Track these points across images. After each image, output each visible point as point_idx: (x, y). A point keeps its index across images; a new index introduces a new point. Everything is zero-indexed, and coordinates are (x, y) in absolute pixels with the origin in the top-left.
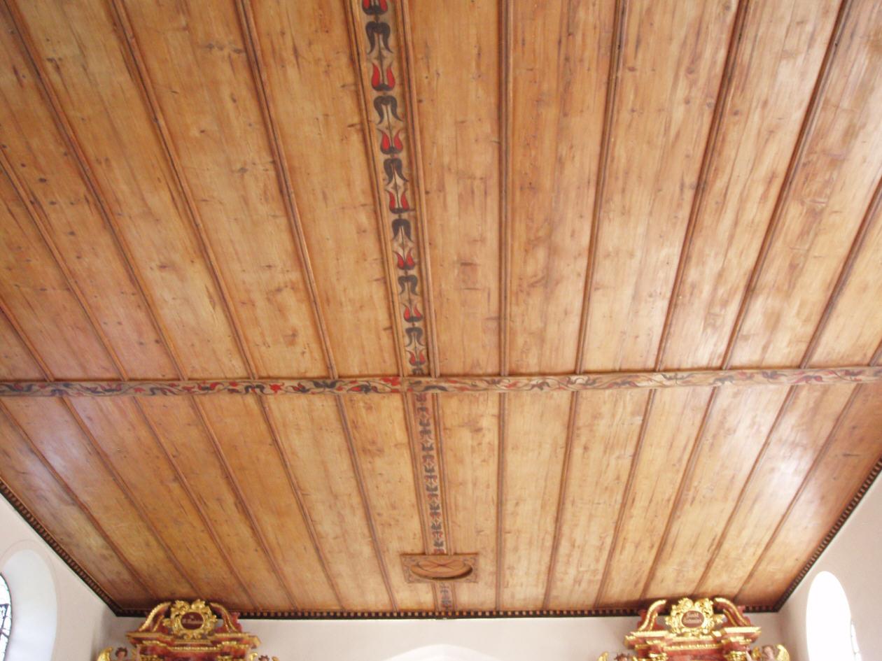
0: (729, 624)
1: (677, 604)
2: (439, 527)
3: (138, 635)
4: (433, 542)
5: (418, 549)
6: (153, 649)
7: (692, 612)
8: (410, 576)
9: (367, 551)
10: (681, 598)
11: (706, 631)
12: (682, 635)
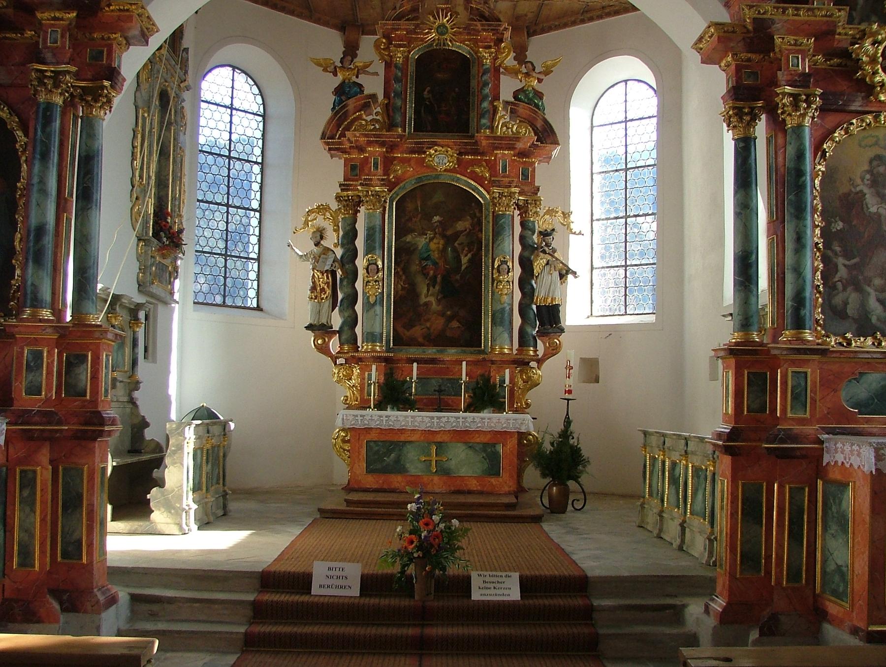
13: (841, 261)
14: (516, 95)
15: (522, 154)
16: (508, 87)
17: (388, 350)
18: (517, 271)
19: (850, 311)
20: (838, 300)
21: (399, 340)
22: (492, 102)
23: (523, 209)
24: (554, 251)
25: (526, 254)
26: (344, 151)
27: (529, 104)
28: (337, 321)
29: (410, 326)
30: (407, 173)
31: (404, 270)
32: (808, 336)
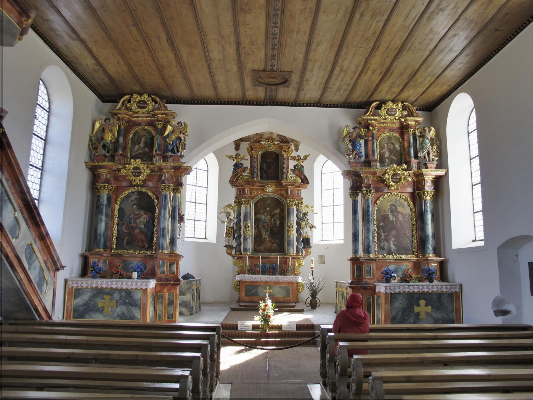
0: (409, 115)
1: (385, 104)
2: (275, 56)
3: (115, 112)
4: (270, 64)
5: (262, 68)
6: (123, 118)
7: (392, 108)
8: (255, 82)
9: (235, 68)
10: (388, 101)
11: (397, 118)
12: (386, 119)
13: (382, 234)
14: (295, 166)
15: (297, 187)
16: (292, 164)
17: (252, 254)
18: (296, 226)
19: (385, 248)
20: (382, 245)
21: (256, 251)
22: (286, 169)
23: (297, 205)
24: (308, 220)
25: (298, 221)
26: (237, 186)
27: (299, 170)
28: (234, 244)
29: (259, 245)
30: (258, 194)
31: (257, 227)
32: (371, 256)
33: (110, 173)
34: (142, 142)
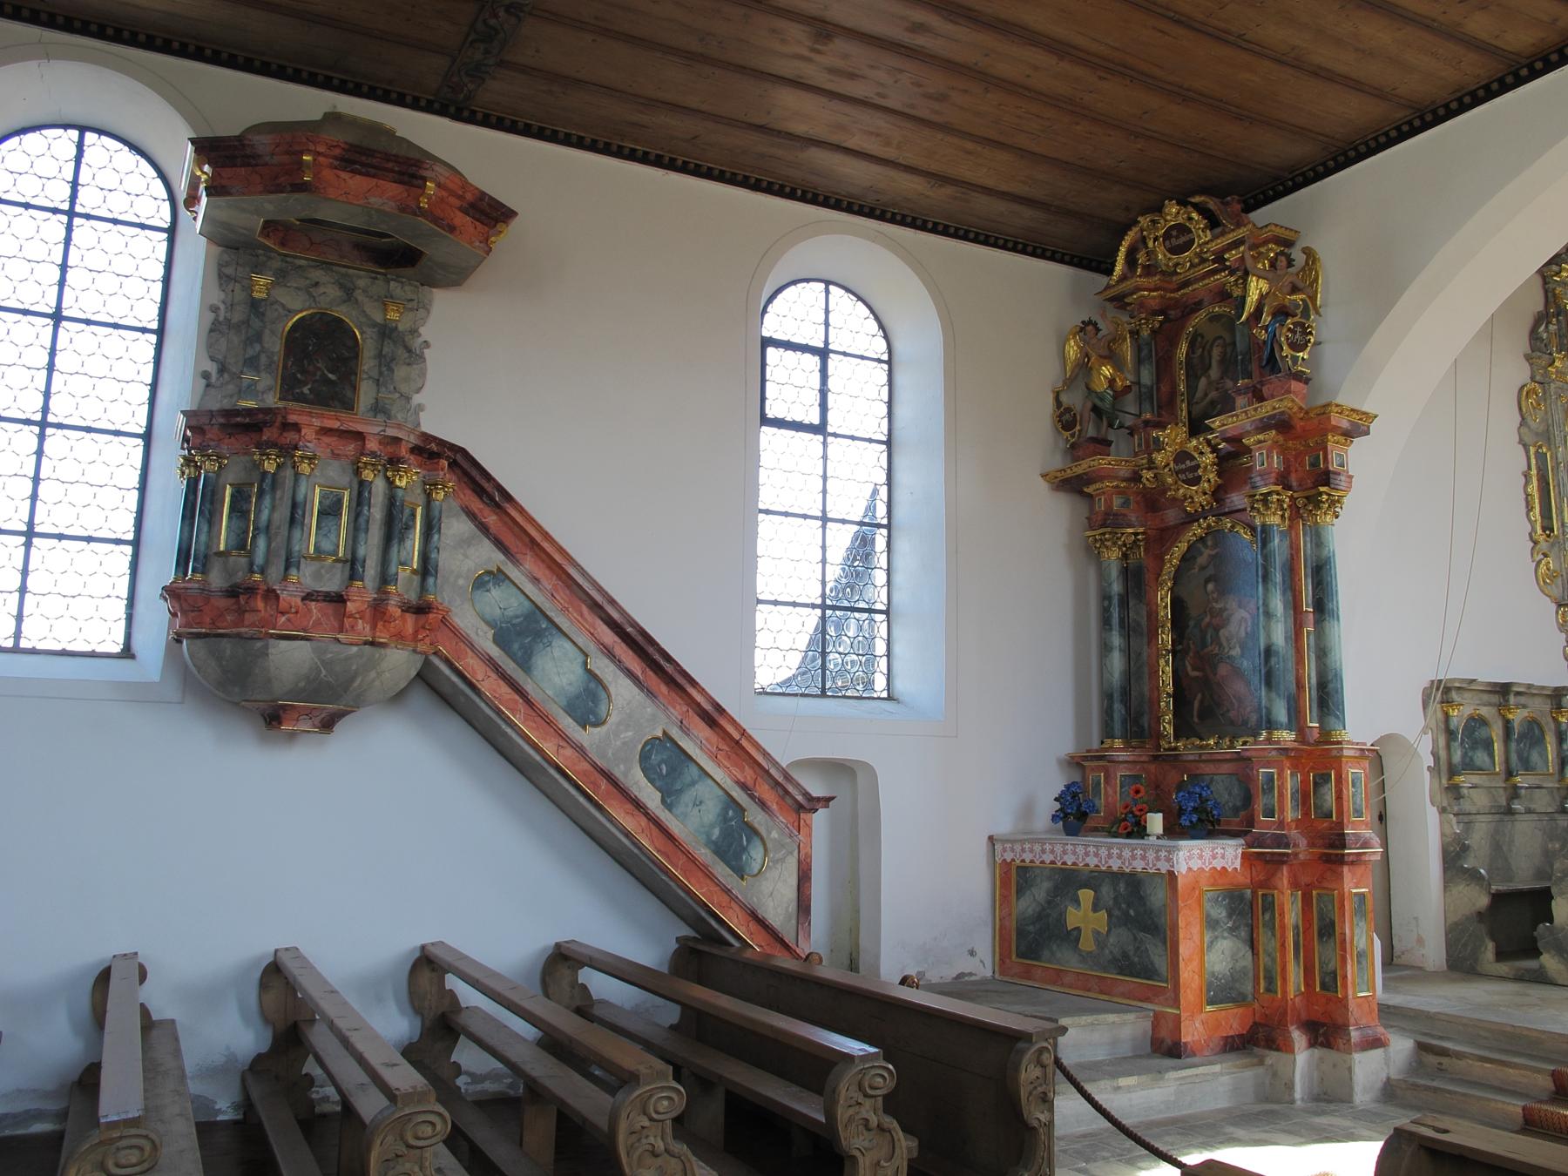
33: (1119, 491)
34: (1214, 364)
